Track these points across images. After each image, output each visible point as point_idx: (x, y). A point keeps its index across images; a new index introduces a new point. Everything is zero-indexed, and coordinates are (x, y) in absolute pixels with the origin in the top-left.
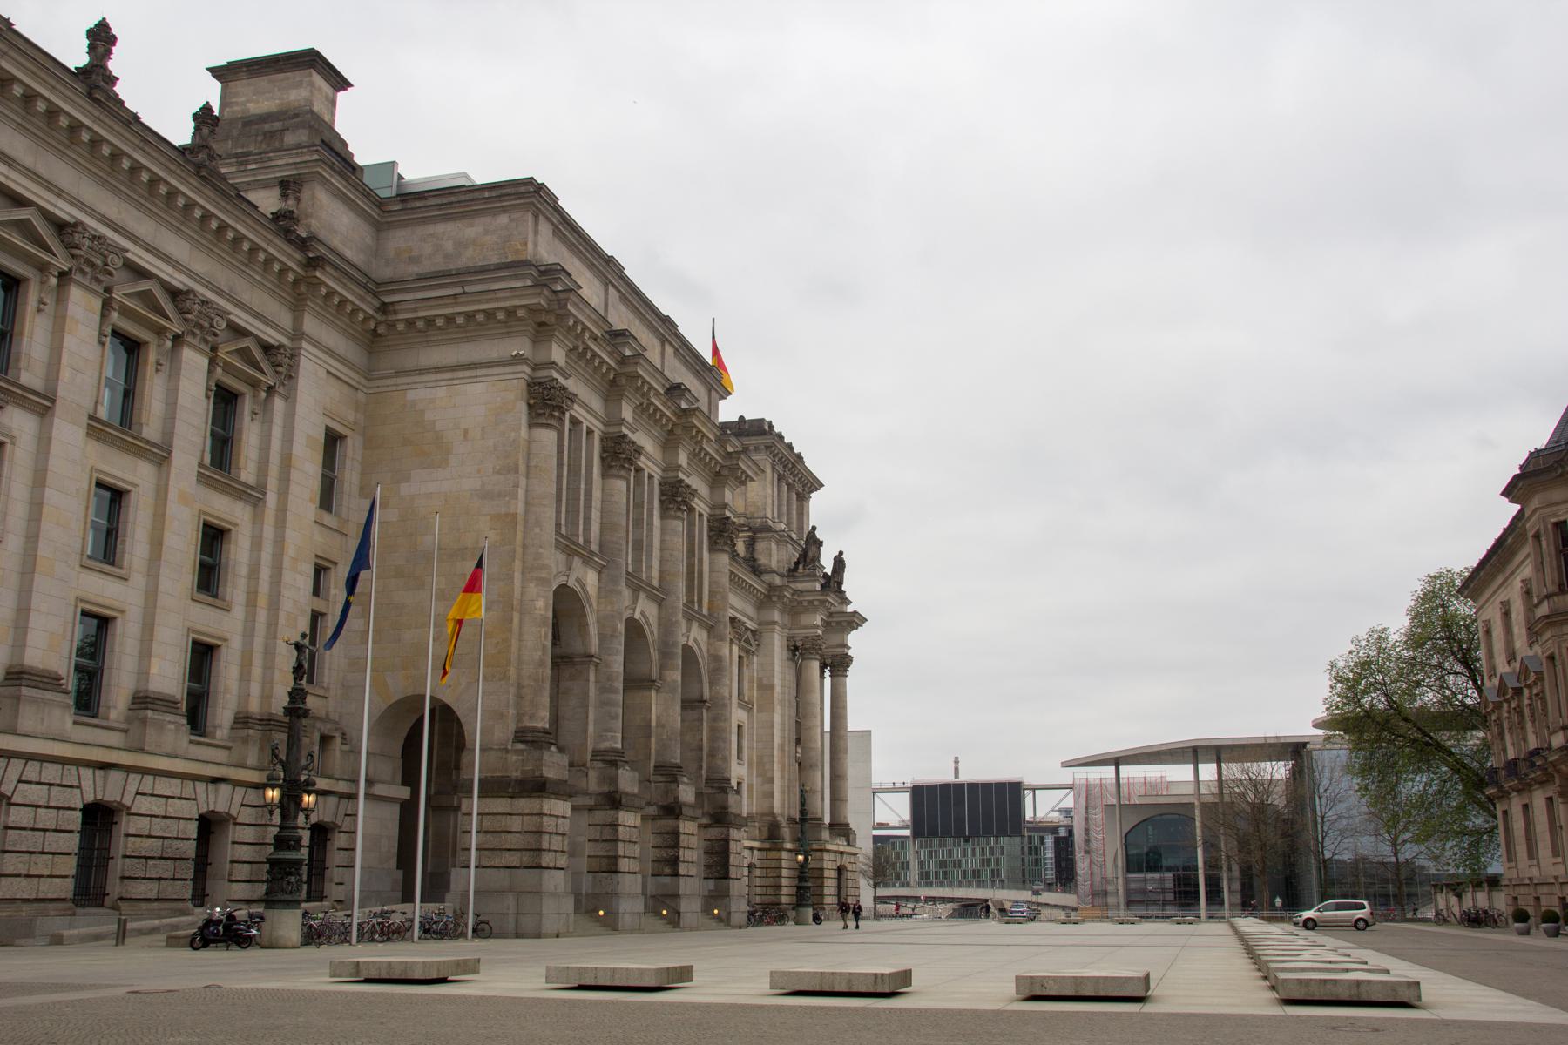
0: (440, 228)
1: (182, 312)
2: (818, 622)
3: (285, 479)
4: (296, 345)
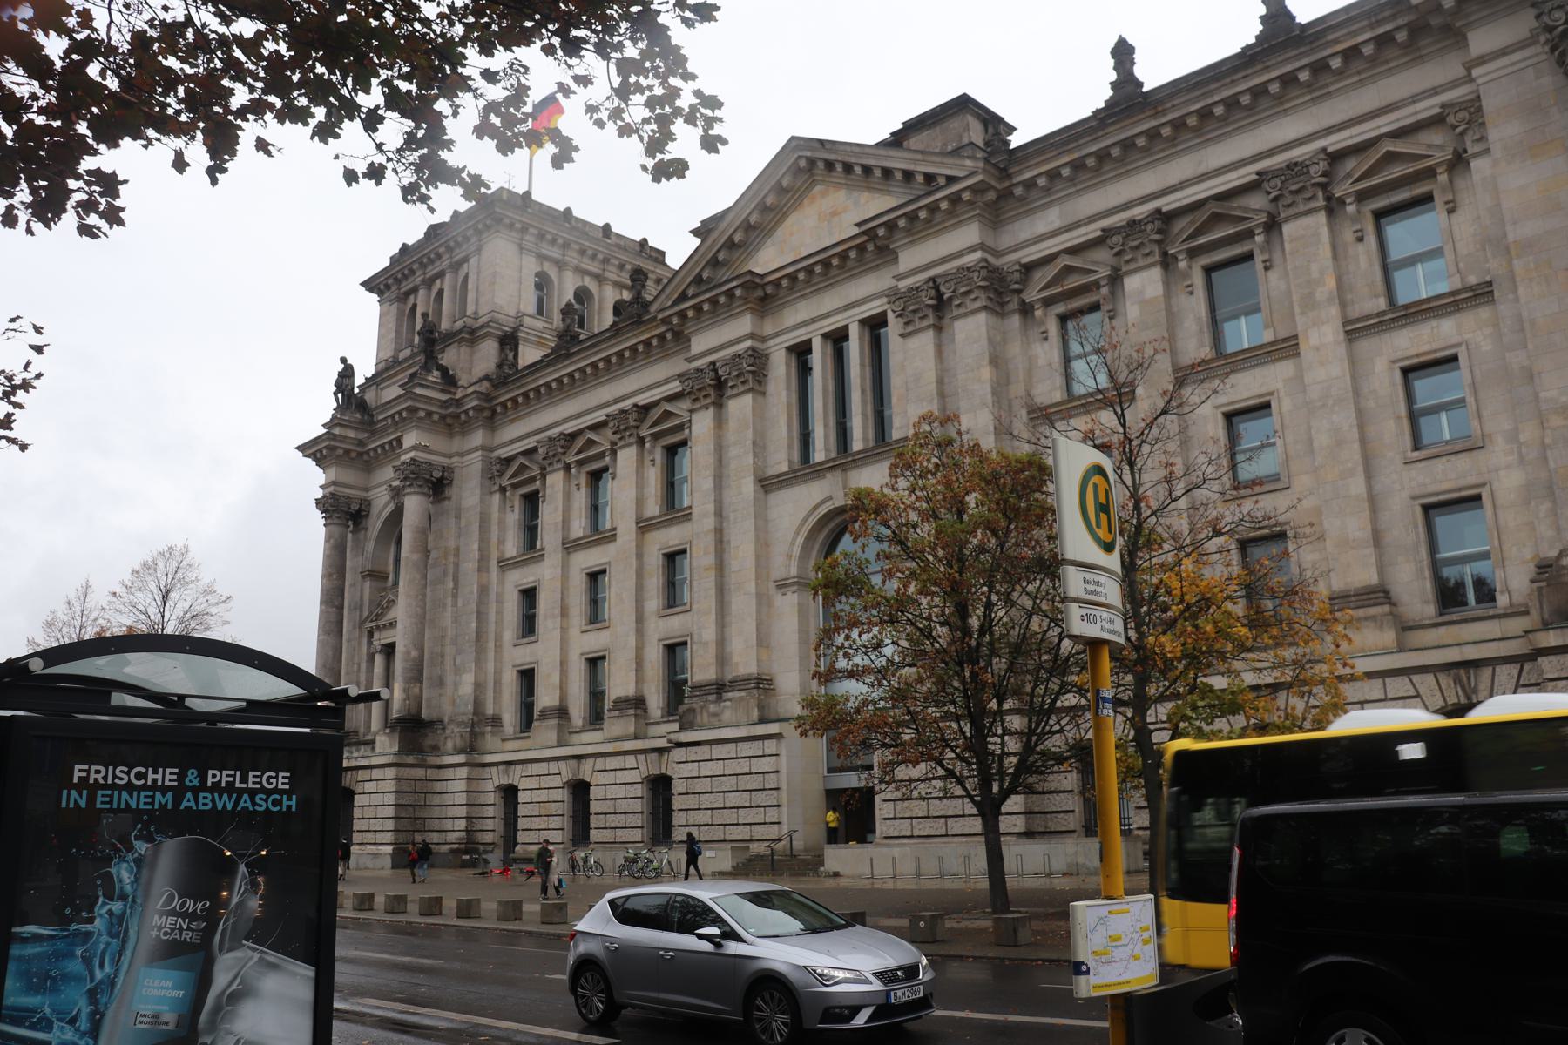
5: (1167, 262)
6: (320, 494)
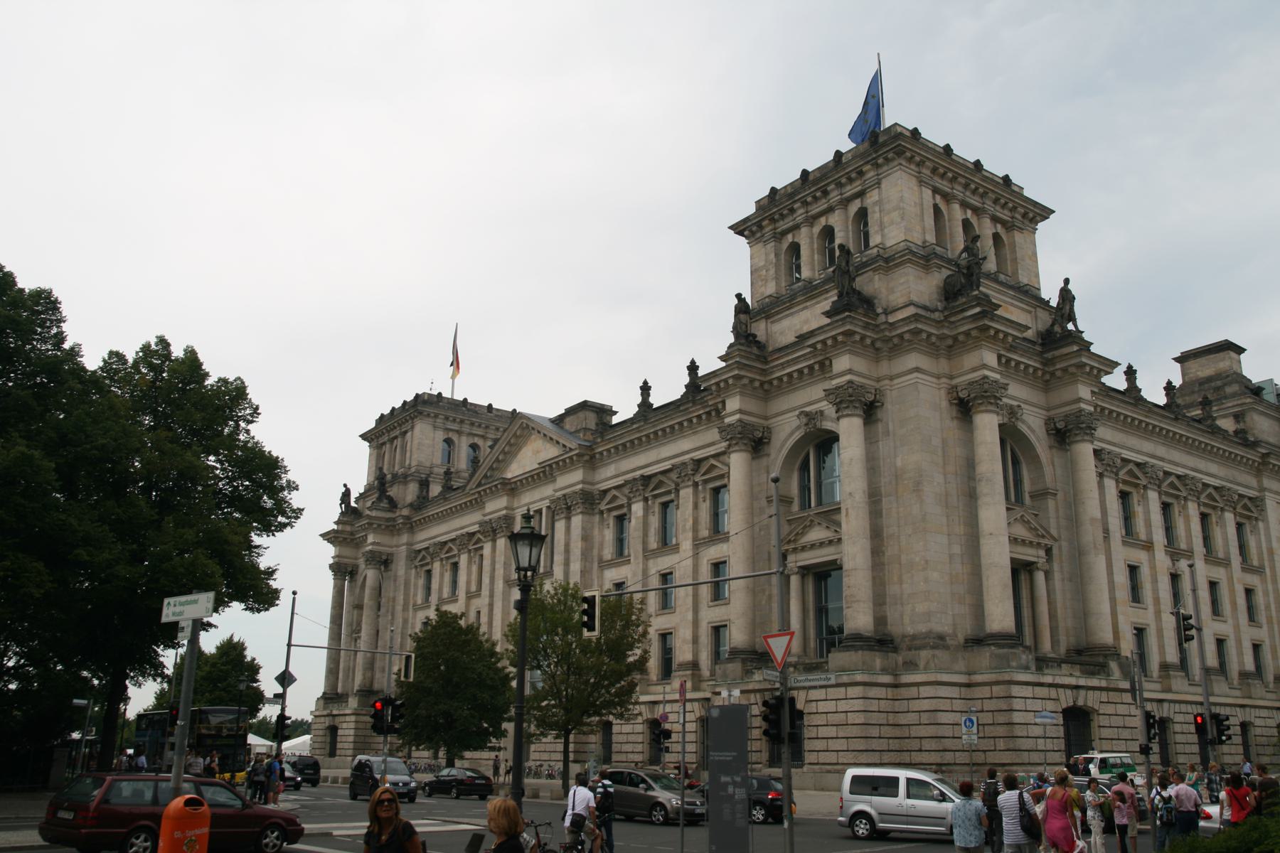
1: (1222, 496)
4: (1262, 494)
5: (646, 500)
6: (331, 561)
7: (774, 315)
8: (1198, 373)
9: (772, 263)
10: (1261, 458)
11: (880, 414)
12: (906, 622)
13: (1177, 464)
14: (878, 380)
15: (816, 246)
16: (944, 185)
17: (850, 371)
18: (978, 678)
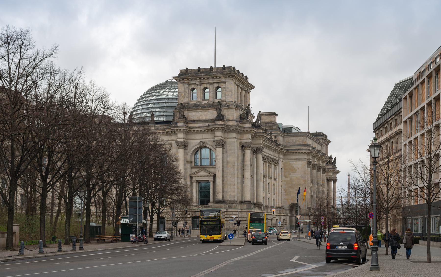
0: (293, 138)
2: (332, 174)
3: (279, 177)
7: (190, 110)
8: (266, 120)
9: (187, 92)
10: (281, 150)
11: (224, 147)
12: (228, 198)
13: (266, 153)
14: (225, 138)
15: (202, 92)
16: (238, 84)
17: (221, 137)
18: (244, 211)
